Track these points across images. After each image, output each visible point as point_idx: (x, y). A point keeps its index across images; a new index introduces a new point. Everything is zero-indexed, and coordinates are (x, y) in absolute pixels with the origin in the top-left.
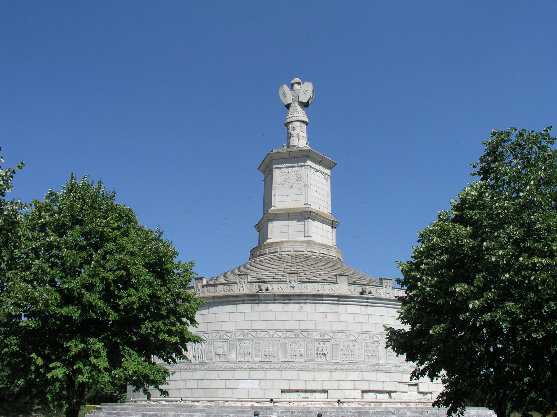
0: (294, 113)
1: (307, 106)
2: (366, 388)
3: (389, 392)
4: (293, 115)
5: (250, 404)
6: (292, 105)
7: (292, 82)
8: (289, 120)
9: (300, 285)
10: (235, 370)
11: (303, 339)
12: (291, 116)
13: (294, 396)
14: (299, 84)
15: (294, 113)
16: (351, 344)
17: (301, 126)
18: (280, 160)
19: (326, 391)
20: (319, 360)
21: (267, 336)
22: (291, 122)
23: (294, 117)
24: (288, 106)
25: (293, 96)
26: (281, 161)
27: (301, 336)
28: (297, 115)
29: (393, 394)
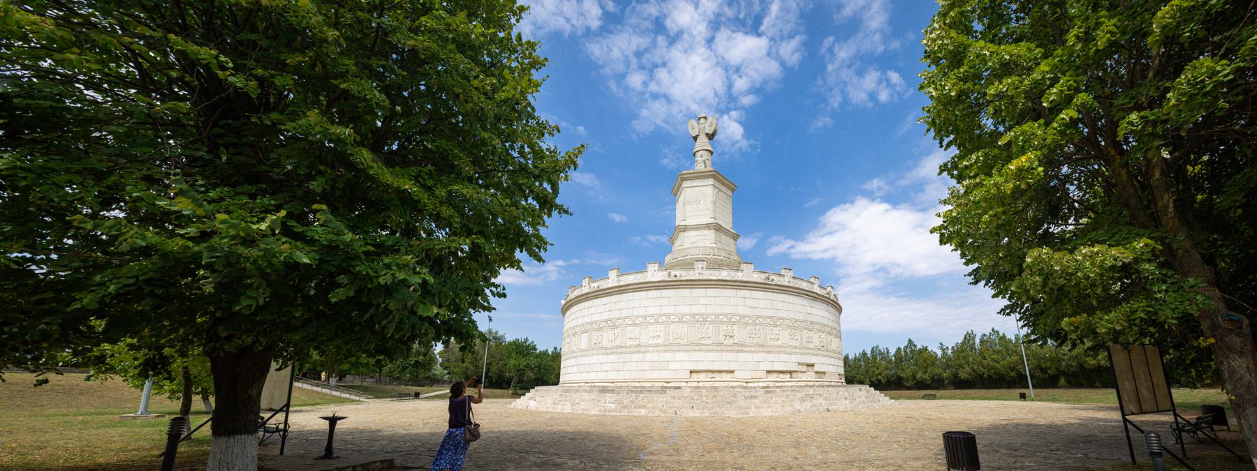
3: (790, 372)
5: (661, 384)
10: (645, 352)
11: (711, 322)
13: (702, 377)
16: (757, 328)
19: (732, 372)
20: (726, 342)
21: (677, 320)
27: (709, 319)
29: (794, 375)
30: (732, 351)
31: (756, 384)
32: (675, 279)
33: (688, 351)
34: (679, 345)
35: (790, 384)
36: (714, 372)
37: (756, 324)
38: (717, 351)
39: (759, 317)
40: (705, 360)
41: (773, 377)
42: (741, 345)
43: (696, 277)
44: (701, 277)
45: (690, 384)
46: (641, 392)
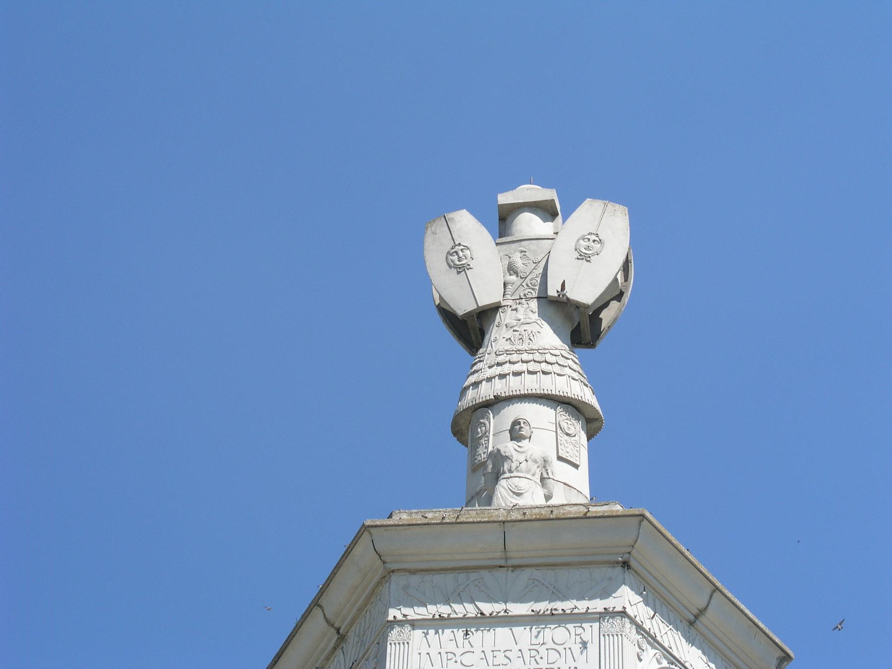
0: (515, 358)
1: (588, 338)
4: (507, 369)
6: (505, 317)
7: (505, 198)
8: (486, 392)
12: (498, 370)
14: (547, 211)
15: (515, 358)
17: (558, 426)
18: (438, 578)
22: (496, 403)
23: (517, 374)
25: (511, 269)
26: (448, 580)
28: (532, 367)
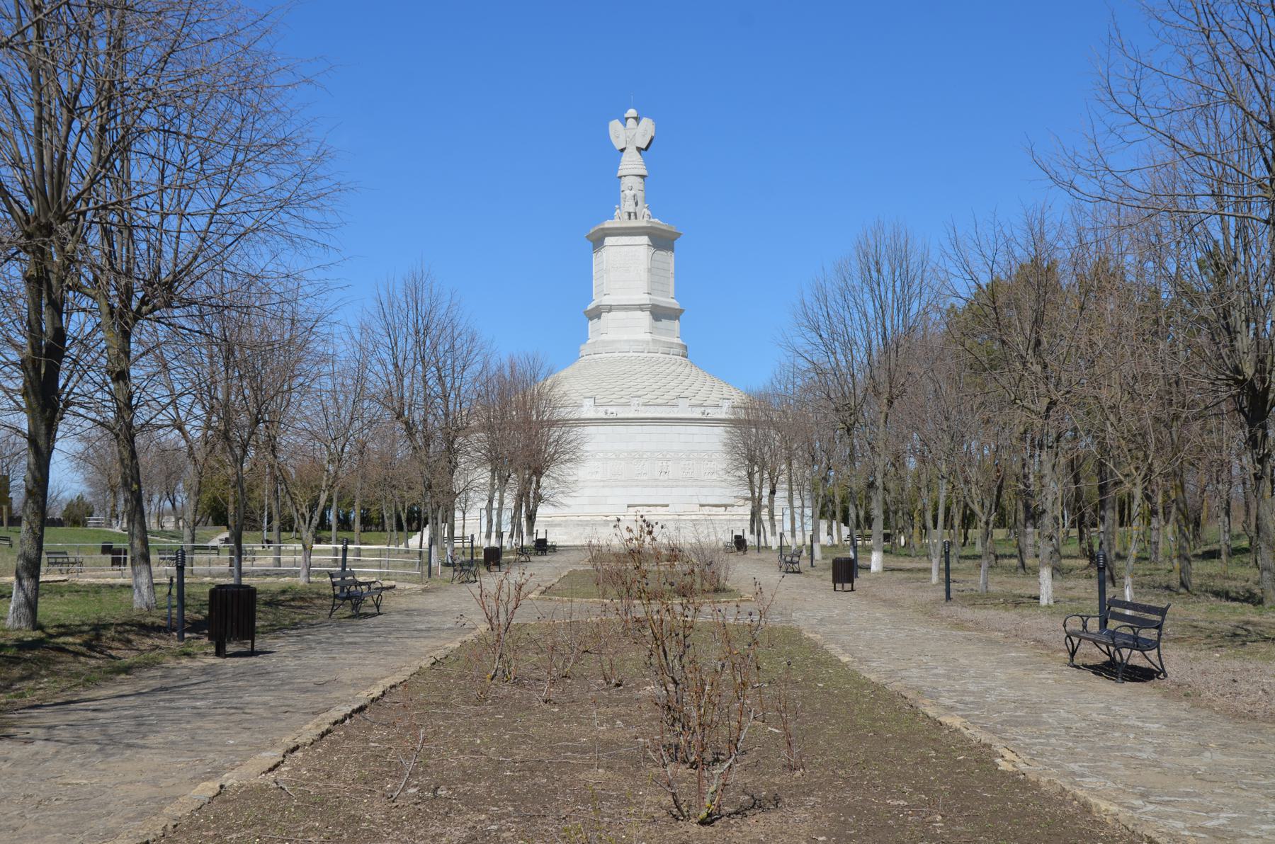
2: (704, 502)
3: (726, 506)
7: (626, 115)
9: (643, 408)
19: (667, 506)
24: (622, 150)
30: (667, 486)
31: (689, 517)
32: (611, 416)
33: (626, 487)
34: (616, 481)
35: (724, 517)
36: (649, 506)
37: (689, 459)
38: (652, 487)
39: (693, 451)
40: (640, 495)
41: (706, 510)
42: (676, 480)
43: (632, 414)
44: (636, 415)
45: (627, 518)
46: (587, 525)
